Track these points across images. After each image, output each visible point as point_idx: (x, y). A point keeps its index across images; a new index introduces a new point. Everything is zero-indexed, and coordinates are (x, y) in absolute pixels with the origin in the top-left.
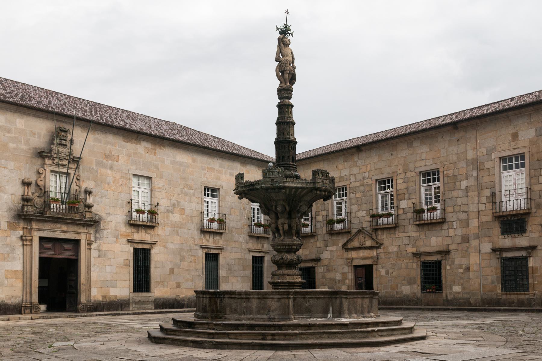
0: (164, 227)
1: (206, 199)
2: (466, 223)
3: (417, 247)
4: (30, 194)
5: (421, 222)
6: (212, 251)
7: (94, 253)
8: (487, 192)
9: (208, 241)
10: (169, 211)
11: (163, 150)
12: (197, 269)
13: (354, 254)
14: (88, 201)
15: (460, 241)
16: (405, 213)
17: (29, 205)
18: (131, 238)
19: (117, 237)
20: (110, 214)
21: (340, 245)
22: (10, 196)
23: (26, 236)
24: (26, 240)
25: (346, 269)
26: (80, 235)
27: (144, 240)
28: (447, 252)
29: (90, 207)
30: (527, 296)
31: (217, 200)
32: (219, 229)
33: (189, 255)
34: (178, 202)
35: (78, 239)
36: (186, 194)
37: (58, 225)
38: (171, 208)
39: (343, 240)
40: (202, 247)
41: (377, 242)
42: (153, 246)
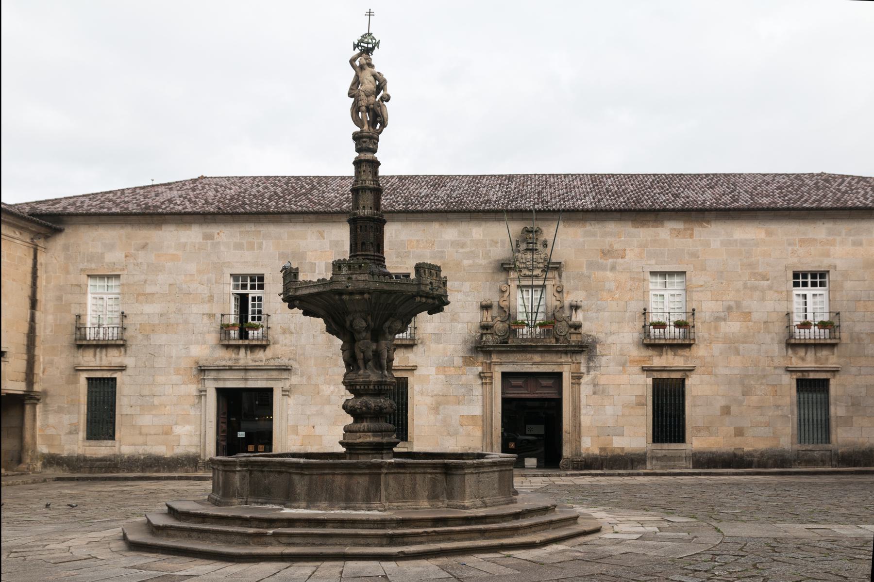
0: (710, 343)
1: (801, 290)
4: (490, 319)
7: (585, 389)
9: (803, 359)
10: (718, 319)
12: (780, 406)
14: (573, 319)
17: (490, 334)
18: (649, 364)
19: (623, 365)
20: (612, 333)
22: (465, 325)
23: (484, 373)
24: (486, 378)
26: (561, 366)
27: (671, 366)
29: (577, 327)
31: (826, 290)
32: (830, 338)
33: (762, 384)
34: (738, 304)
35: (559, 371)
36: (754, 288)
37: (529, 356)
38: (722, 314)
40: (788, 370)
42: (688, 373)
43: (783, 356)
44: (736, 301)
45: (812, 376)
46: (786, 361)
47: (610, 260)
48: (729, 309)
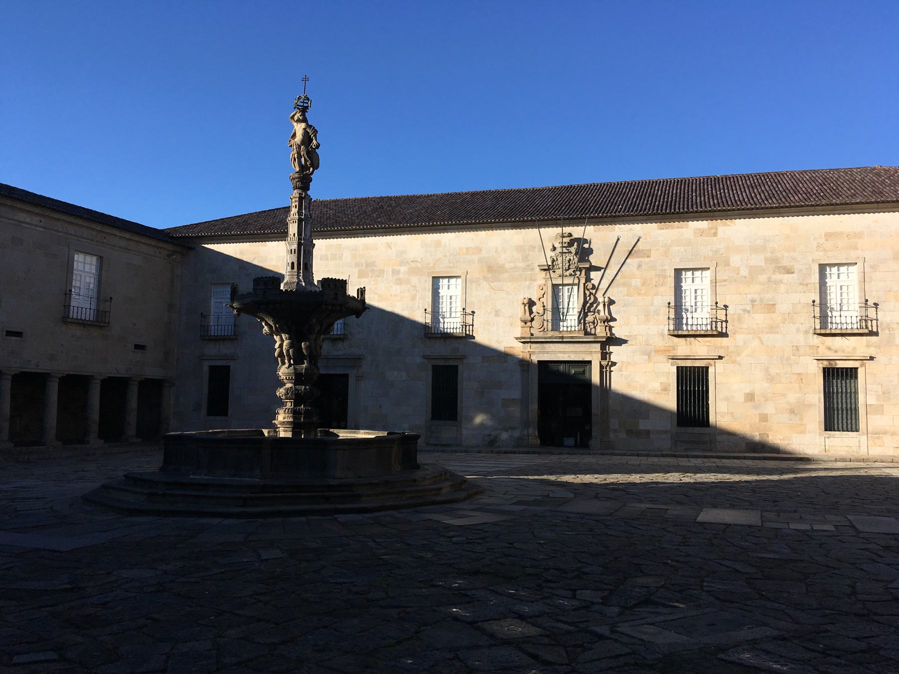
11: (729, 225)
19: (649, 355)
27: (695, 355)
45: (840, 364)
46: (811, 351)
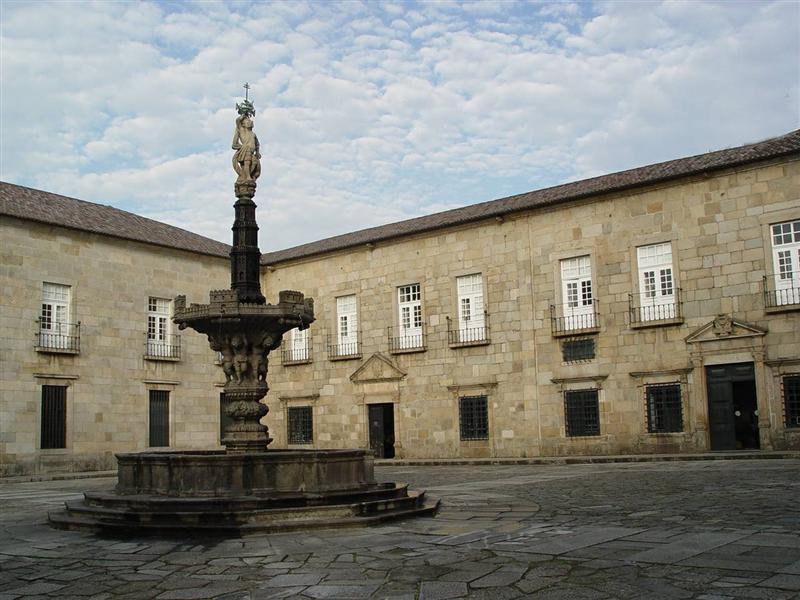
2: (518, 346)
3: (454, 378)
5: (458, 345)
6: (160, 388)
8: (545, 305)
9: (154, 373)
13: (367, 388)
15: (511, 369)
16: (437, 332)
19: (17, 371)
21: (348, 376)
25: (356, 410)
28: (495, 385)
30: (598, 441)
36: (121, 308)
38: (98, 329)
39: (350, 368)
41: (399, 372)
42: (71, 381)
43: (142, 370)
44: (110, 319)
45: (160, 388)
47: (9, 266)
48: (103, 324)
